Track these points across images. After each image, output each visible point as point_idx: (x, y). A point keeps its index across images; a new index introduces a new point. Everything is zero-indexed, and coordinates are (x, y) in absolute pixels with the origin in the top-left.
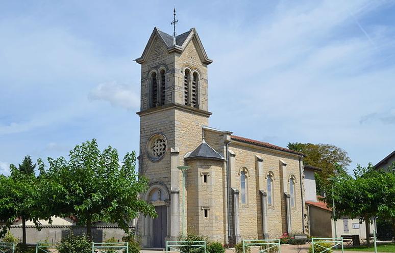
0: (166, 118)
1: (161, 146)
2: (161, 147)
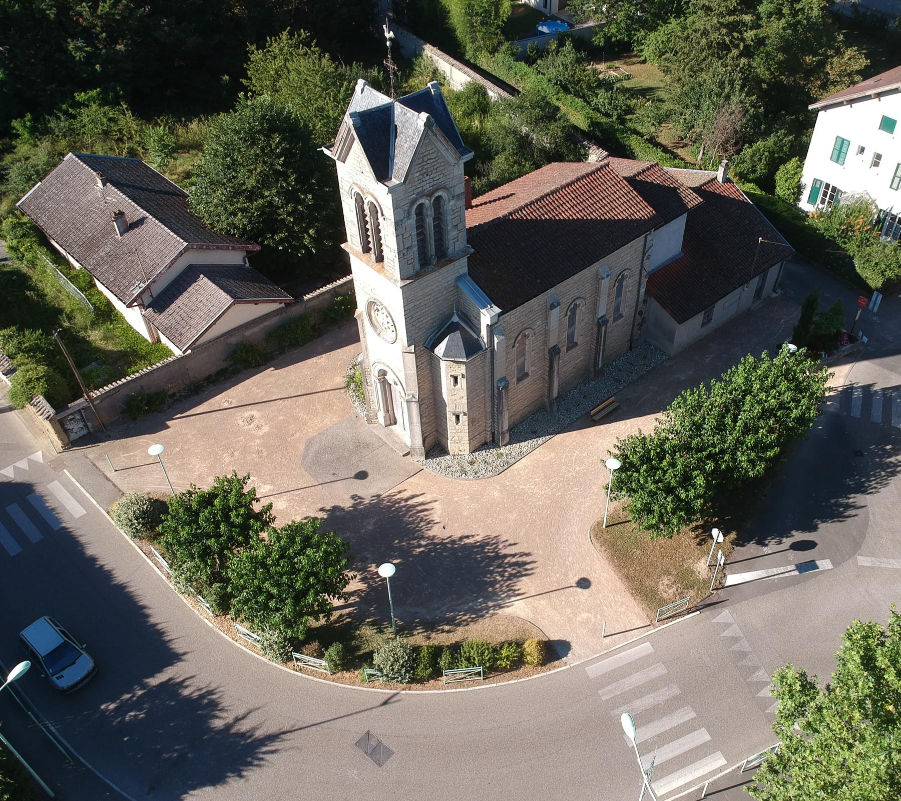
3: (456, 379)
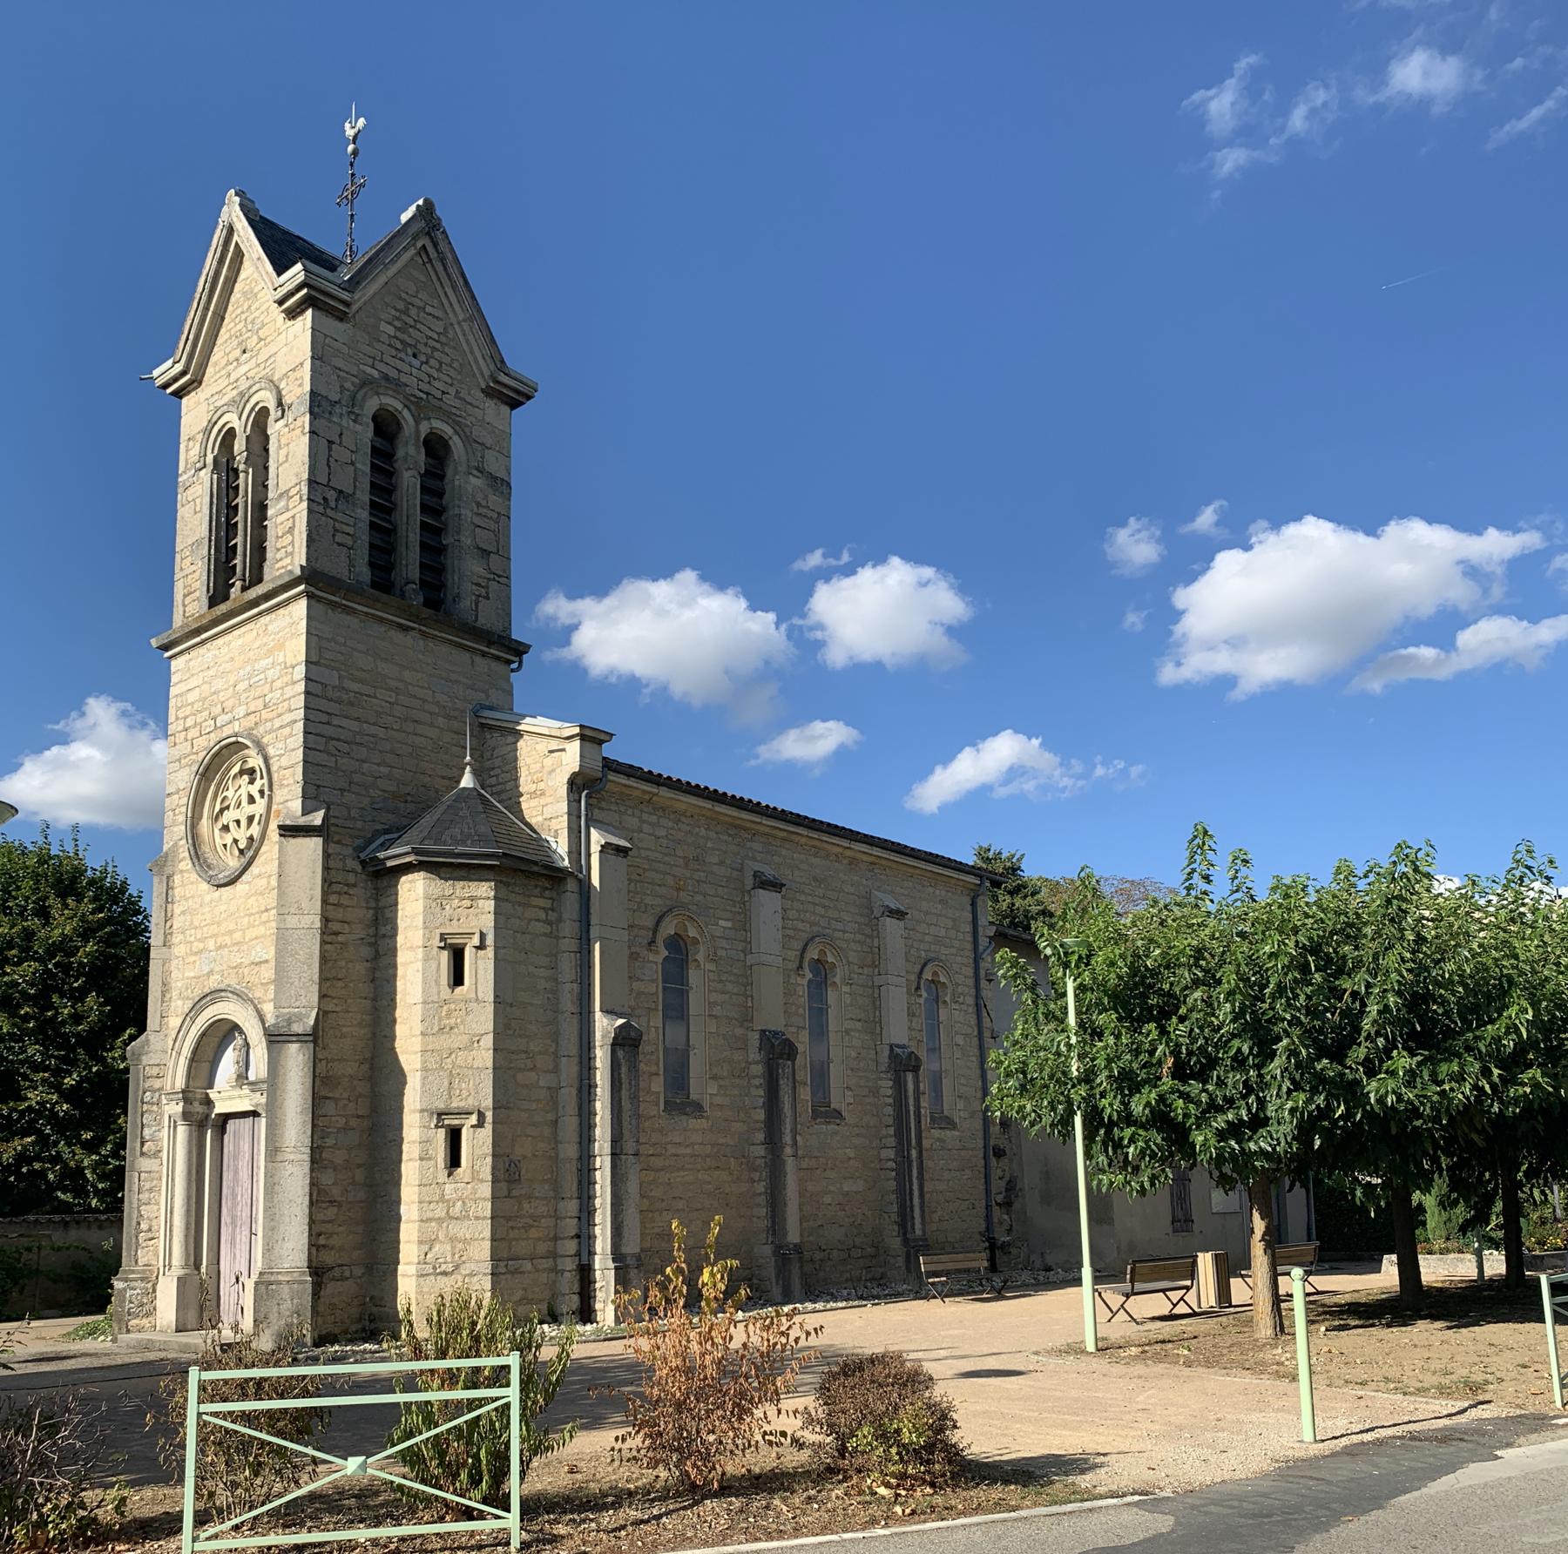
0: (270, 652)
1: (251, 800)
2: (249, 810)
3: (457, 955)
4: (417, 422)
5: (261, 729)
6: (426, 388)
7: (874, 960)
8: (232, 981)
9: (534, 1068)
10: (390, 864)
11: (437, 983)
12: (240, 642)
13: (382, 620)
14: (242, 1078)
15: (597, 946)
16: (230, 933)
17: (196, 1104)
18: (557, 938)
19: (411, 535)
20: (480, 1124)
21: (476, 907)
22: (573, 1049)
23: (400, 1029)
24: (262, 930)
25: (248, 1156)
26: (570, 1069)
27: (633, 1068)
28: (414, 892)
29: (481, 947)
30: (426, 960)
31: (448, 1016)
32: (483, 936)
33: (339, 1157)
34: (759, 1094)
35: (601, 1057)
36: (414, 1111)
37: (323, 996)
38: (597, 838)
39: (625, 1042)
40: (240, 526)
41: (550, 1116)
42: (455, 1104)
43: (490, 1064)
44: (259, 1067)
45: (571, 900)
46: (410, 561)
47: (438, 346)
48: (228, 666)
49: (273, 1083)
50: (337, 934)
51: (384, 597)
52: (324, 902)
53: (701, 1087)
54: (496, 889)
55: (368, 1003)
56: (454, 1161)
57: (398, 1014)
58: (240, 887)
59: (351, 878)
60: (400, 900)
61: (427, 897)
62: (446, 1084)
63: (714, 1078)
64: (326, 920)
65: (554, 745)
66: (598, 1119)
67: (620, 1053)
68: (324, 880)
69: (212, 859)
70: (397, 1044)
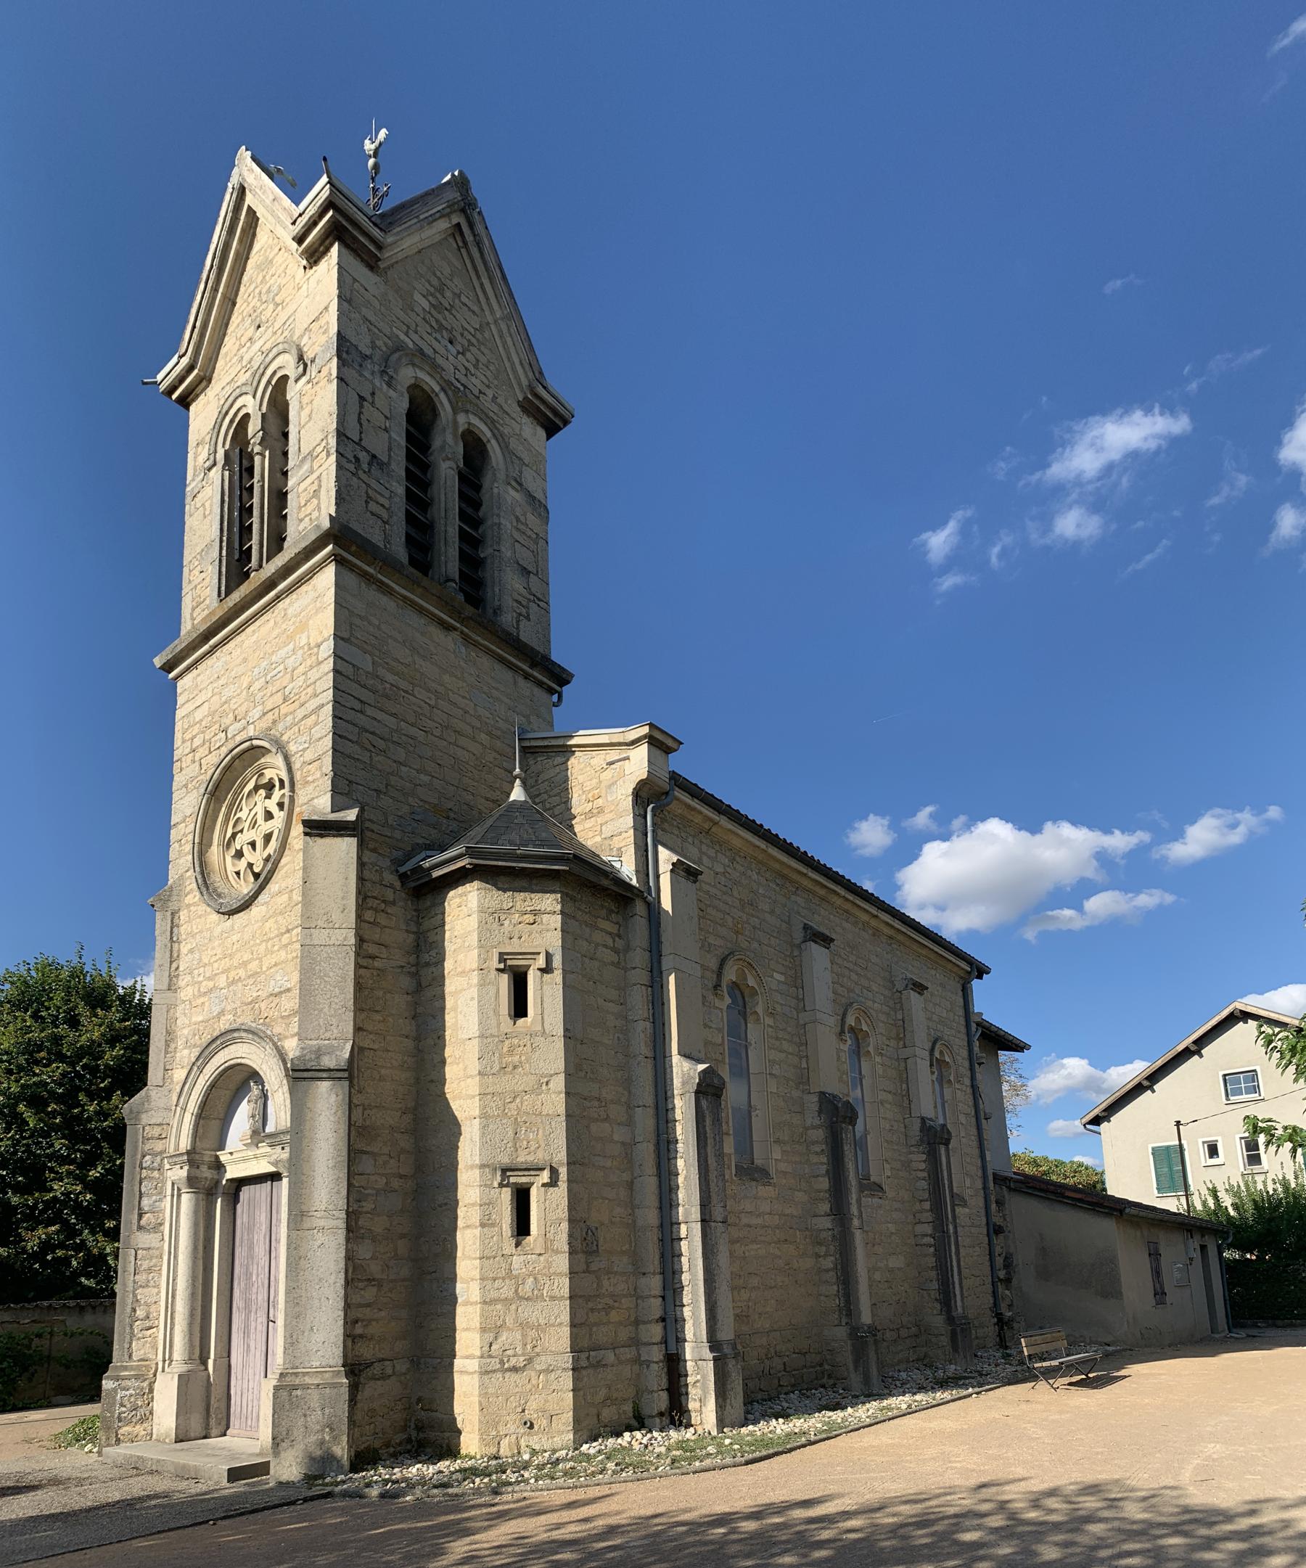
1: (269, 816)
4: (455, 412)
5: (280, 727)
6: (463, 380)
7: (902, 1031)
8: (246, 1019)
9: (607, 1119)
10: (436, 874)
11: (496, 1013)
12: (254, 638)
13: (421, 611)
14: (258, 1134)
15: (672, 979)
16: (245, 964)
17: (204, 1168)
18: (626, 970)
19: (450, 529)
20: (553, 1183)
21: (540, 923)
22: (649, 1099)
23: (451, 1071)
24: (283, 953)
25: (264, 1228)
26: (645, 1121)
27: (717, 1120)
28: (466, 909)
29: (547, 970)
30: (482, 984)
31: (511, 1051)
32: (549, 957)
33: (379, 1225)
34: (821, 1162)
35: (683, 1108)
36: (472, 1167)
37: (358, 1029)
38: (666, 858)
39: (708, 1090)
40: (256, 512)
41: (626, 1176)
42: (523, 1158)
43: (562, 1109)
44: (280, 1115)
45: (640, 924)
46: (449, 556)
47: (474, 341)
48: (241, 669)
49: (297, 1134)
50: (373, 957)
51: (425, 582)
52: (359, 917)
53: (768, 1153)
54: (563, 902)
55: (409, 1044)
56: (522, 1227)
57: (448, 1052)
58: (256, 911)
59: (390, 895)
60: (447, 919)
61: (482, 910)
62: (511, 1134)
63: (777, 1141)
64: (361, 940)
65: (614, 754)
66: (681, 1180)
67: (704, 1103)
68: (359, 892)
69: (222, 887)
70: (448, 1089)
